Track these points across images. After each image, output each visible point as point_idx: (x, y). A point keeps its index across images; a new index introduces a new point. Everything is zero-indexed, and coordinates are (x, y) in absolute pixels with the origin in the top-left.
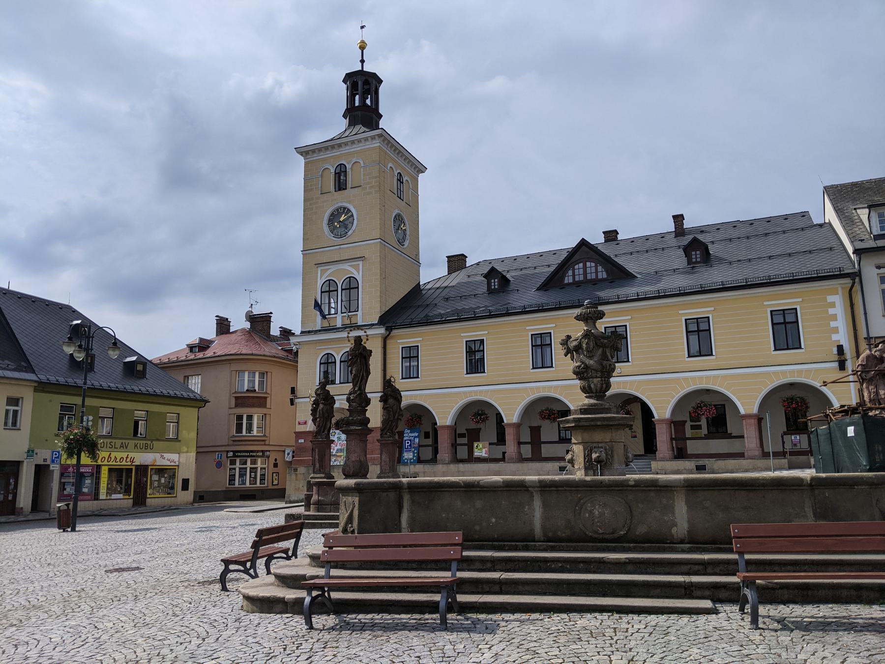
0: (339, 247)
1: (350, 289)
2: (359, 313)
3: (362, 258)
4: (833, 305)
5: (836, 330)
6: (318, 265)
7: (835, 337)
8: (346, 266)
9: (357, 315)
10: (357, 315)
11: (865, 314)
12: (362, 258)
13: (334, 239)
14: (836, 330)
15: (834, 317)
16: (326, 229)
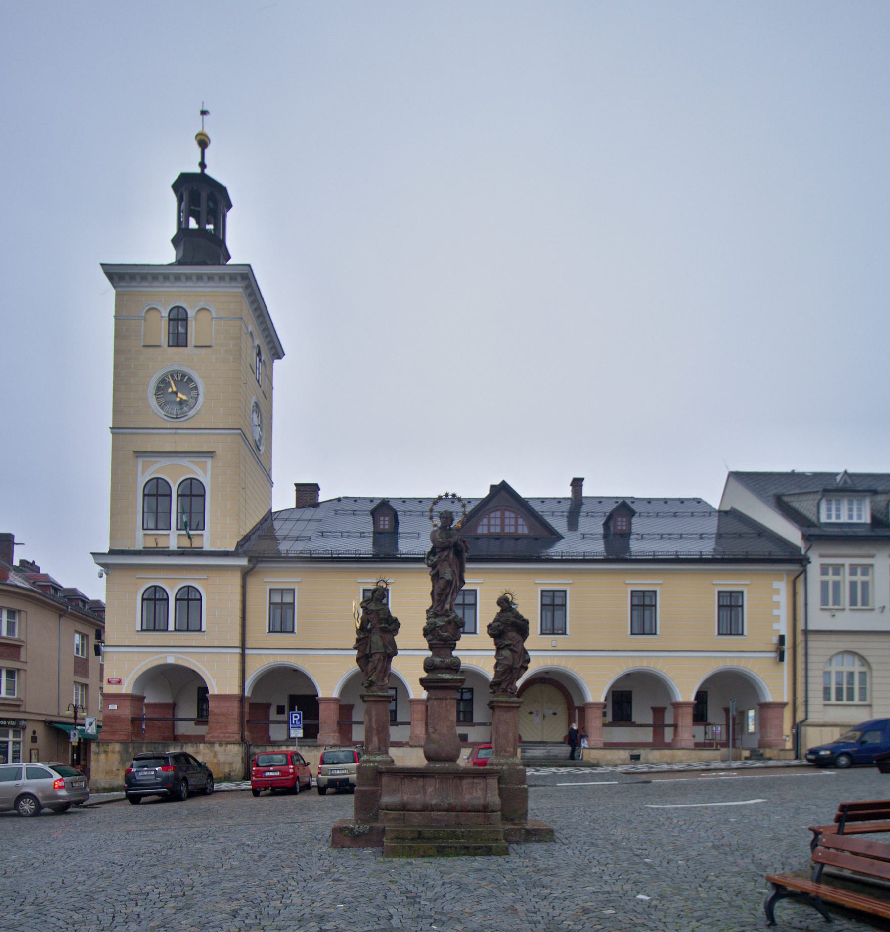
0: (173, 431)
1: (191, 495)
2: (206, 533)
3: (210, 454)
4: (777, 592)
5: (777, 619)
6: (139, 454)
7: (776, 626)
8: (185, 462)
9: (202, 535)
10: (202, 535)
11: (806, 605)
12: (210, 454)
13: (166, 418)
14: (777, 619)
15: (777, 605)
16: (153, 402)
